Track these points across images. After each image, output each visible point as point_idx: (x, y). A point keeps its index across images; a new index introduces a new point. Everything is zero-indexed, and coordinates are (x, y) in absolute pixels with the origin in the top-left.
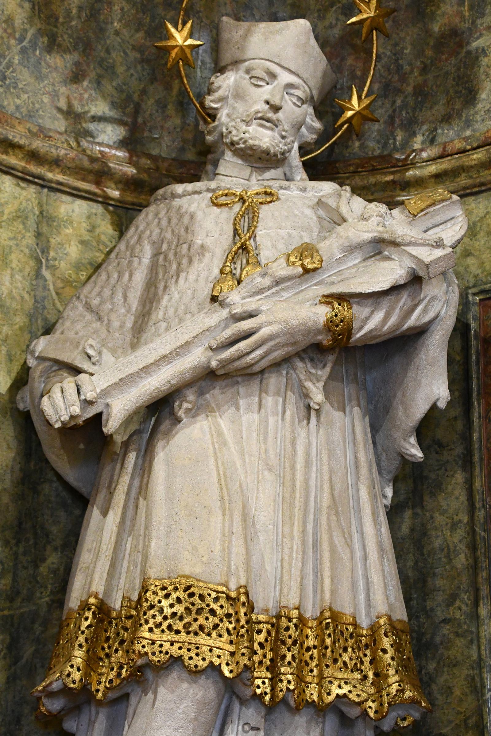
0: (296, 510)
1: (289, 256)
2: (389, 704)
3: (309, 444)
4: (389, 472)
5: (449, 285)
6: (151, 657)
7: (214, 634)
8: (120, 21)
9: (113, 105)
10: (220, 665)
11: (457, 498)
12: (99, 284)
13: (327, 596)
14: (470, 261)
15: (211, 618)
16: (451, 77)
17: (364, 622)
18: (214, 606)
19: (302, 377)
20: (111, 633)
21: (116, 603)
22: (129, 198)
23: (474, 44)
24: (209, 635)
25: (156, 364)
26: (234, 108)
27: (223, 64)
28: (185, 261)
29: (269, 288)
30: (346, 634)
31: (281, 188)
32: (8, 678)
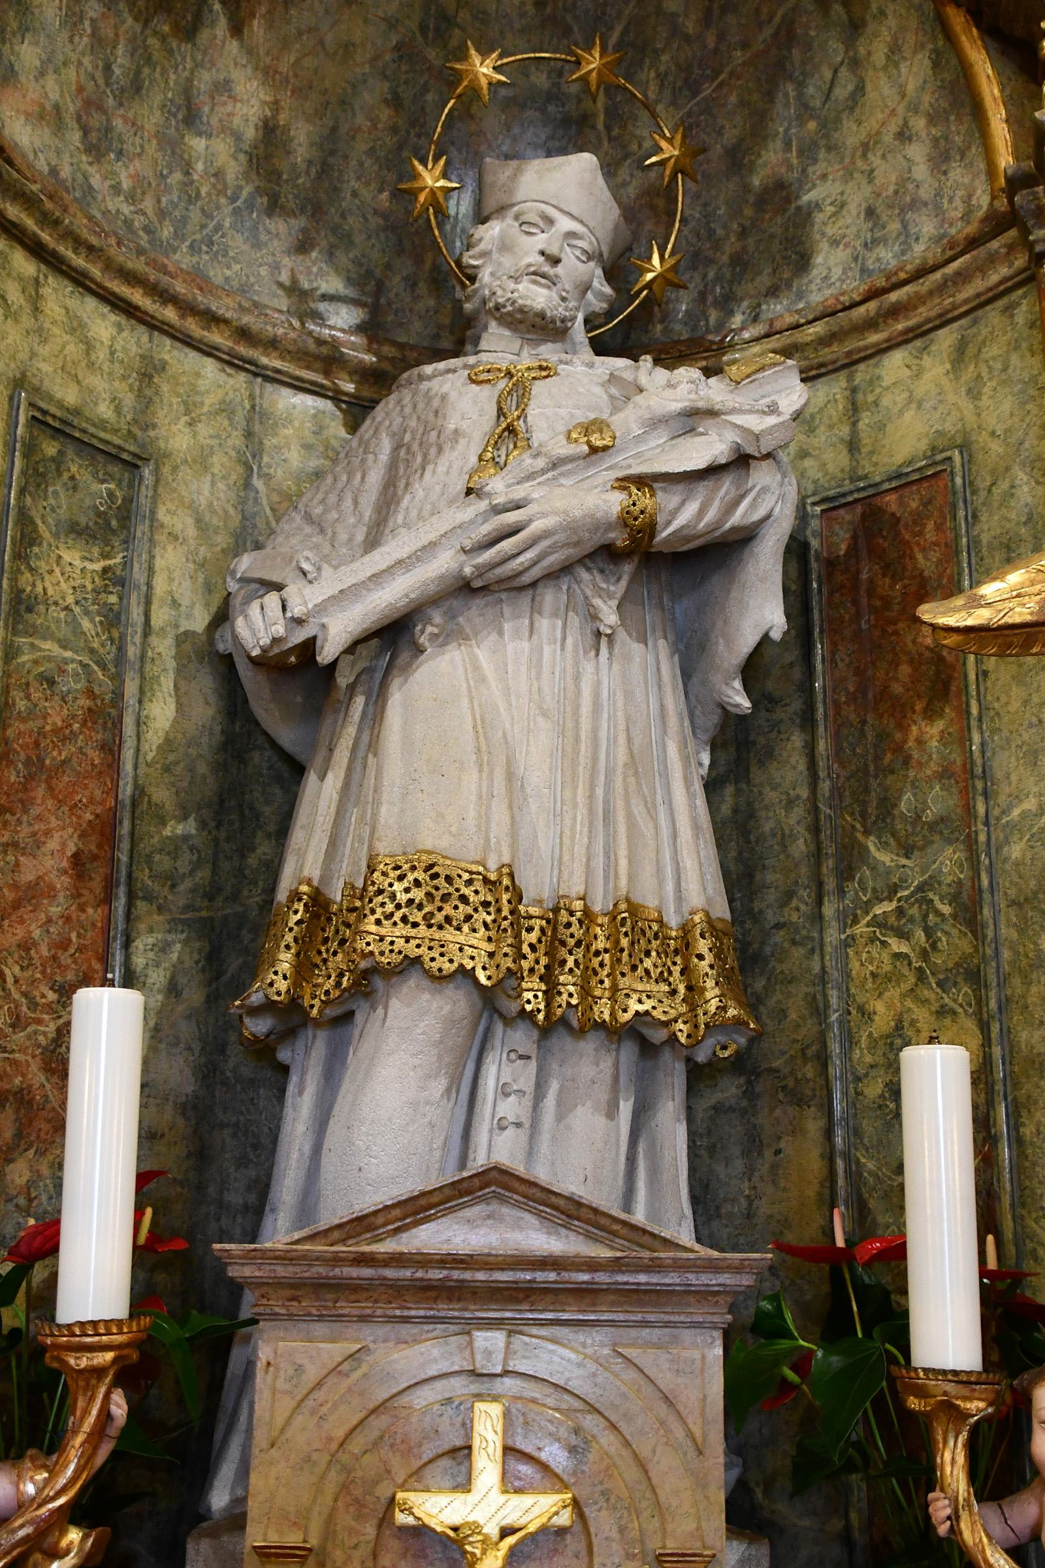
0: (581, 768)
1: (569, 432)
2: (707, 1025)
3: (598, 683)
4: (706, 730)
5: (784, 476)
6: (379, 958)
7: (466, 928)
8: (358, 178)
9: (349, 281)
10: (473, 969)
11: (794, 768)
12: (323, 489)
13: (623, 882)
14: (808, 463)
15: (461, 907)
16: (777, 241)
17: (673, 921)
18: (466, 891)
19: (589, 592)
20: (330, 933)
21: (336, 894)
22: (367, 393)
23: (805, 198)
24: (459, 928)
25: (389, 571)
26: (500, 264)
27: (486, 213)
28: (433, 451)
29: (543, 472)
30: (649, 934)
31: (561, 362)
32: (208, 996)
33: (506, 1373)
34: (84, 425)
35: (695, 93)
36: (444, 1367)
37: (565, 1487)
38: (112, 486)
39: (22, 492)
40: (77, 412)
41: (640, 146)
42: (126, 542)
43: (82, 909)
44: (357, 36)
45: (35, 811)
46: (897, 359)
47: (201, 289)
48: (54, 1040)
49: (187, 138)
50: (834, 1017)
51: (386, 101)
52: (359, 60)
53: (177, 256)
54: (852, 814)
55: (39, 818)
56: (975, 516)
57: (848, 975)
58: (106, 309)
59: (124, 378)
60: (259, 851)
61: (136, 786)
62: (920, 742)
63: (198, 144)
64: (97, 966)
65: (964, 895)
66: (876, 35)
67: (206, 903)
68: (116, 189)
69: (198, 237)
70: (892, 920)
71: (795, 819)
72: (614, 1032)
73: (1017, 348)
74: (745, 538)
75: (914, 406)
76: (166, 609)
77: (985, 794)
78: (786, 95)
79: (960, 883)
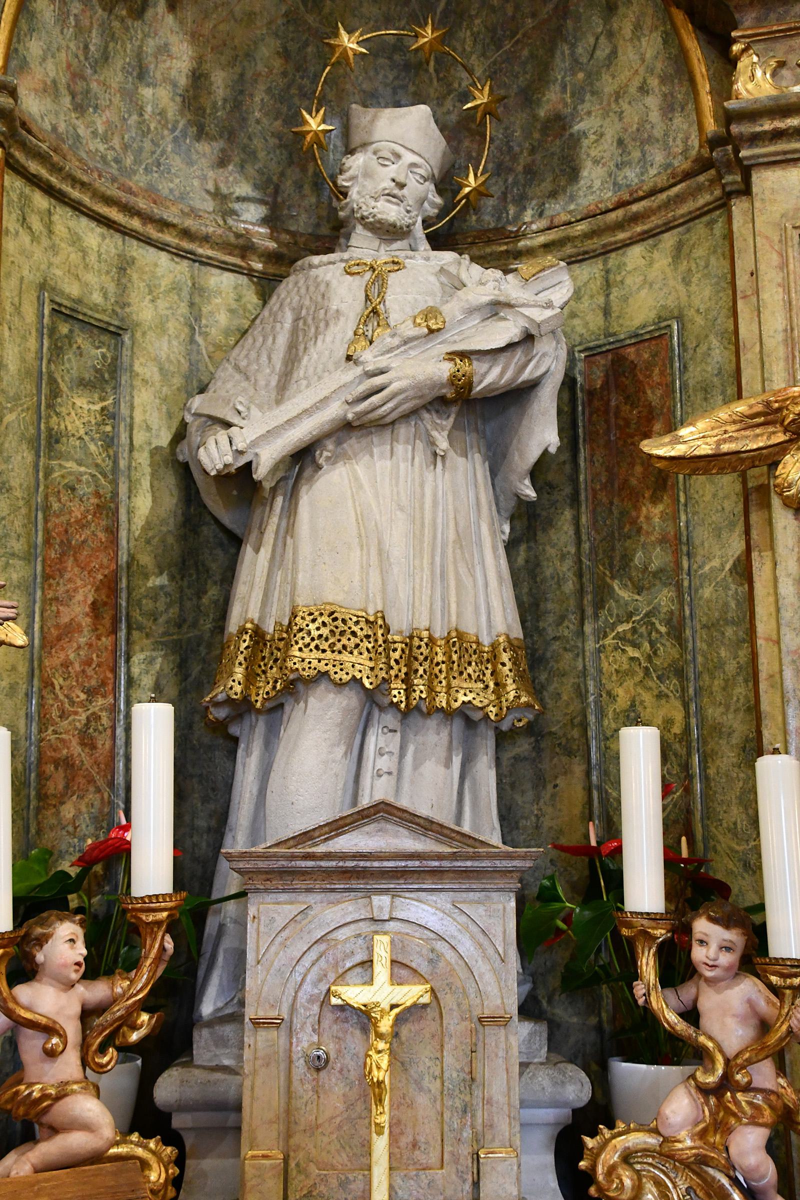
0: (425, 545)
1: (415, 318)
2: (508, 708)
3: (436, 487)
5: (558, 343)
6: (302, 673)
7: (356, 652)
8: (260, 110)
9: (256, 187)
13: (454, 618)
14: (576, 322)
15: (352, 638)
16: (556, 157)
17: (486, 641)
18: (355, 628)
19: (429, 427)
20: (266, 653)
22: (271, 270)
24: (351, 653)
26: (364, 186)
28: (322, 325)
29: (398, 347)
31: (407, 257)
33: (391, 919)
34: (85, 310)
35: (499, 47)
36: (356, 916)
37: (427, 982)
38: (104, 350)
39: (49, 361)
40: (79, 301)
41: (460, 85)
42: (115, 388)
43: (99, 638)
45: (67, 576)
46: (636, 251)
47: (155, 202)
48: (86, 725)
49: (140, 90)
50: (591, 699)
51: (278, 53)
52: (259, 24)
53: (137, 178)
54: (604, 565)
55: (70, 580)
56: (685, 367)
57: (600, 671)
58: (93, 225)
59: (108, 273)
60: (210, 593)
61: (129, 554)
62: (648, 518)
63: (147, 92)
64: (110, 675)
65: (675, 620)
66: (625, 16)
67: (176, 630)
68: (95, 134)
69: (149, 161)
70: (629, 636)
71: (566, 568)
72: (448, 714)
73: (715, 252)
74: (533, 386)
75: (647, 286)
76: (142, 433)
78: (563, 53)
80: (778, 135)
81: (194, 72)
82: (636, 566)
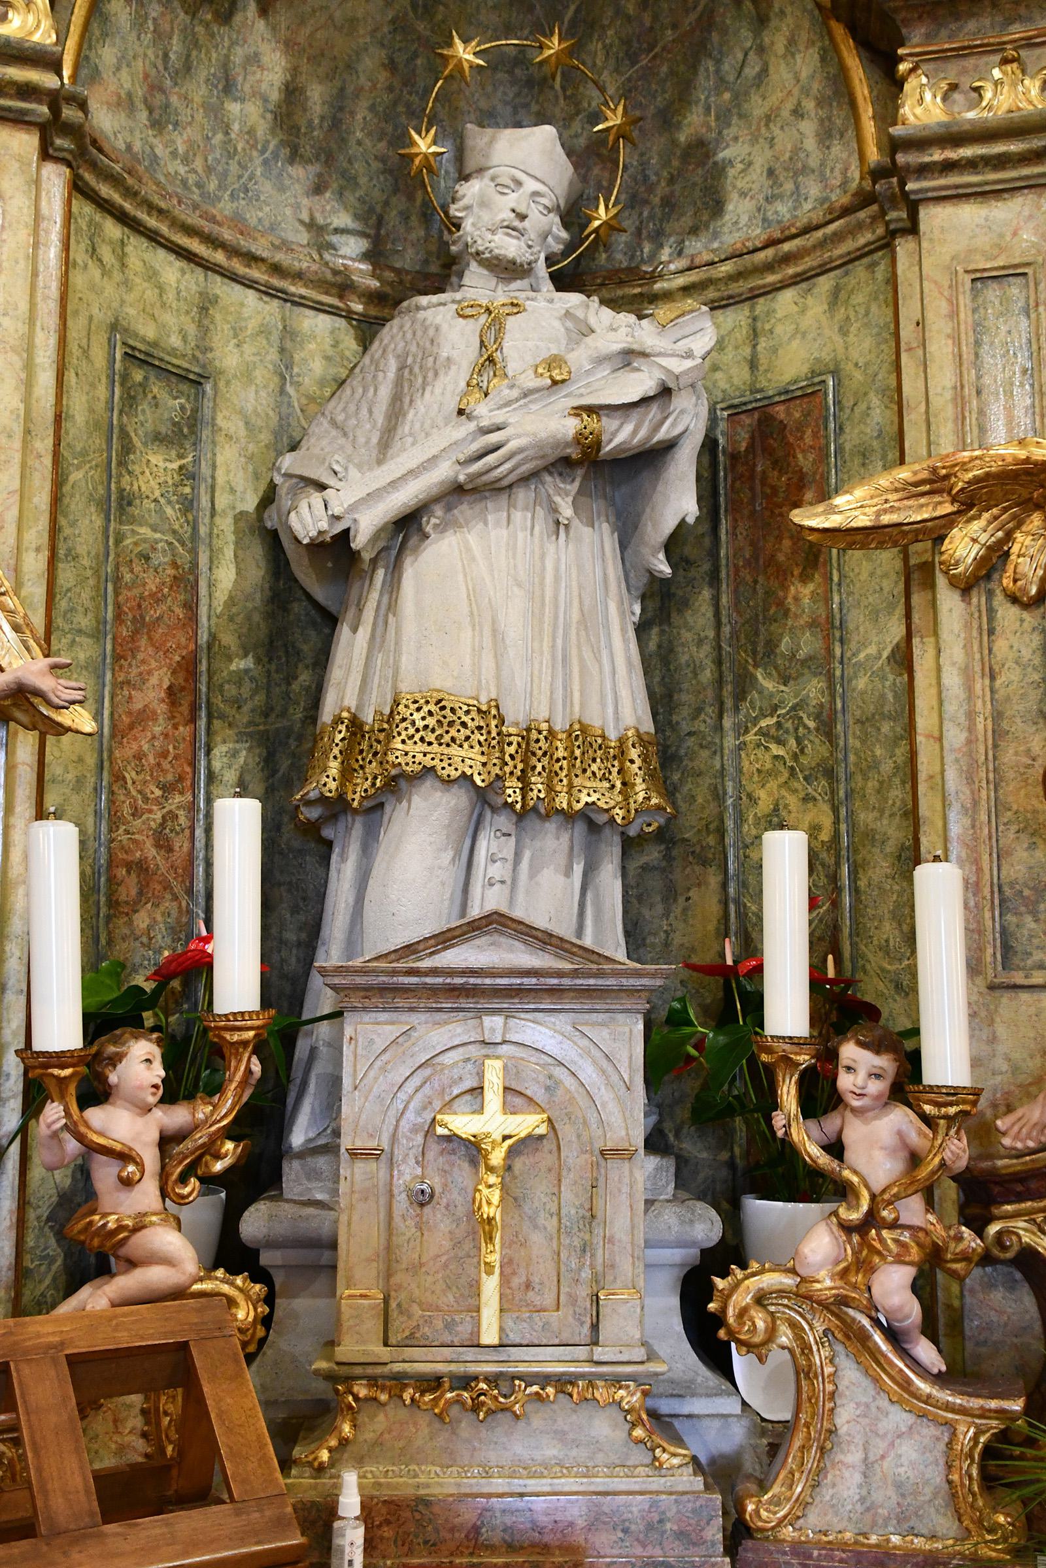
1: (537, 367)
3: (558, 560)
4: (637, 589)
5: (698, 398)
7: (466, 745)
9: (356, 217)
12: (344, 399)
13: (577, 708)
14: (719, 375)
16: (698, 188)
17: (613, 735)
18: (465, 719)
20: (364, 746)
21: (368, 717)
22: (373, 312)
23: (721, 155)
24: (461, 746)
25: (403, 478)
28: (431, 374)
30: (595, 746)
33: (504, 1042)
34: (162, 355)
36: (466, 1039)
37: (544, 1111)
39: (121, 412)
40: (155, 344)
43: (175, 727)
44: (360, 13)
45: (140, 656)
46: (788, 295)
47: (242, 233)
50: (730, 801)
51: (383, 65)
52: (362, 32)
53: (221, 205)
55: (143, 662)
56: (841, 428)
57: (740, 771)
58: (172, 257)
59: (187, 312)
60: (301, 678)
61: (210, 634)
62: (797, 599)
63: (234, 108)
64: (188, 769)
66: (778, 29)
69: (236, 186)
70: (773, 731)
71: (704, 654)
72: (569, 817)
73: (876, 299)
74: (669, 446)
76: (226, 495)
77: (842, 641)
78: (707, 70)
79: (822, 705)
80: (948, 167)
81: (287, 85)
82: (783, 655)
